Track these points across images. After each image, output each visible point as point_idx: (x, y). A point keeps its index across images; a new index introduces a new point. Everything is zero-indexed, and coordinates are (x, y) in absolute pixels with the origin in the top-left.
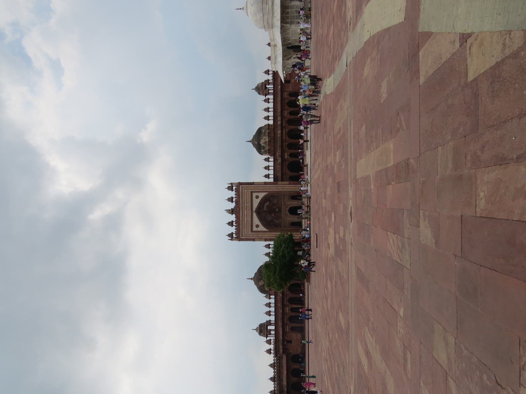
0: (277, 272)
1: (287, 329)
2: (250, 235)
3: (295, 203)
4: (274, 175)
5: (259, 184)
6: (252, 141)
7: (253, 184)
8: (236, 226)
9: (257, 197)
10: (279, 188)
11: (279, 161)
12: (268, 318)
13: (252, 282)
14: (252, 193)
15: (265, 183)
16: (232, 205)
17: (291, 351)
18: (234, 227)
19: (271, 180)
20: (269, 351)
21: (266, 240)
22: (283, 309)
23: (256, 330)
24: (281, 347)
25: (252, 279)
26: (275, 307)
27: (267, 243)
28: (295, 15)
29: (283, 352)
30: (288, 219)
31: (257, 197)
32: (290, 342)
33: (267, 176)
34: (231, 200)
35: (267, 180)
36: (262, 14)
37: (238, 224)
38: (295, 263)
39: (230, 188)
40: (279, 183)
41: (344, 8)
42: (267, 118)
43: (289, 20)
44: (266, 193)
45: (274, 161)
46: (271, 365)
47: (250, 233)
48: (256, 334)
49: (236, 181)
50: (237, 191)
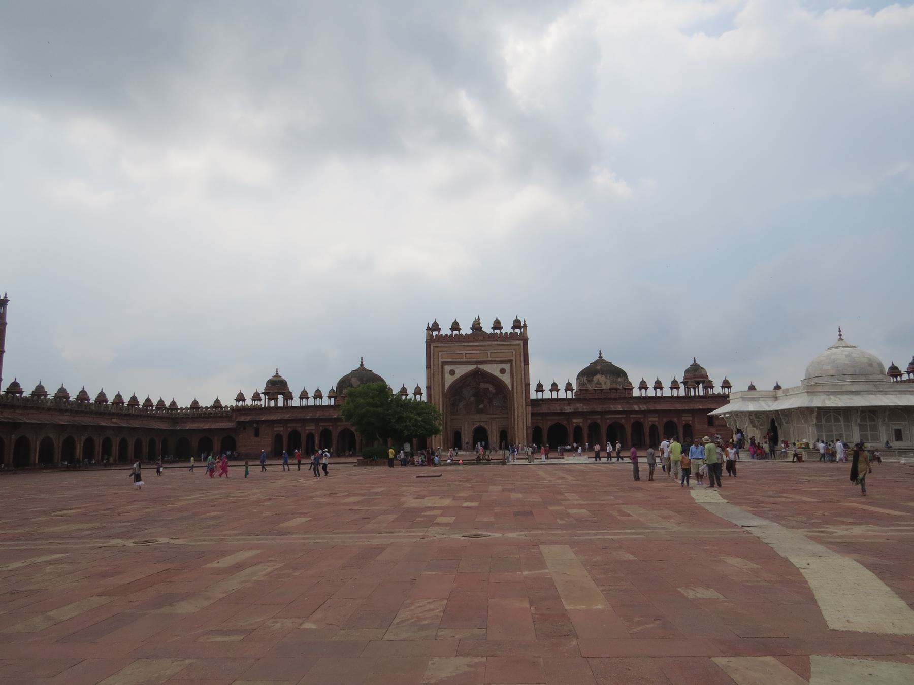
1: (279, 429)
3: (494, 437)
4: (543, 400)
6: (601, 360)
8: (451, 335)
9: (503, 371)
11: (568, 409)
12: (296, 394)
13: (356, 366)
14: (510, 361)
15: (527, 385)
16: (487, 328)
19: (533, 395)
20: (240, 398)
21: (429, 388)
22: (313, 420)
23: (277, 375)
24: (248, 418)
25: (362, 365)
26: (315, 407)
27: (424, 391)
28: (835, 433)
29: (239, 423)
31: (503, 371)
32: (257, 434)
33: (540, 388)
34: (497, 325)
35: (533, 387)
36: (832, 373)
37: (456, 339)
38: (389, 440)
39: (517, 324)
40: (529, 409)
41: (849, 520)
42: (643, 386)
43: (823, 422)
44: (510, 386)
45: (566, 400)
46: (217, 402)
47: (441, 360)
48: (270, 376)
49: (529, 335)
50: (513, 336)
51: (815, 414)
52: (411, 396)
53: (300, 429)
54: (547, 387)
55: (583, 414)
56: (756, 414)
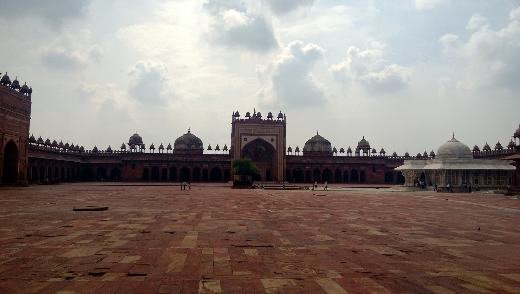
6: (318, 136)
7: (285, 137)
9: (272, 140)
14: (277, 135)
15: (285, 148)
31: (272, 140)
34: (270, 115)
39: (280, 115)
44: (276, 148)
47: (240, 133)
49: (287, 121)
55: (311, 164)
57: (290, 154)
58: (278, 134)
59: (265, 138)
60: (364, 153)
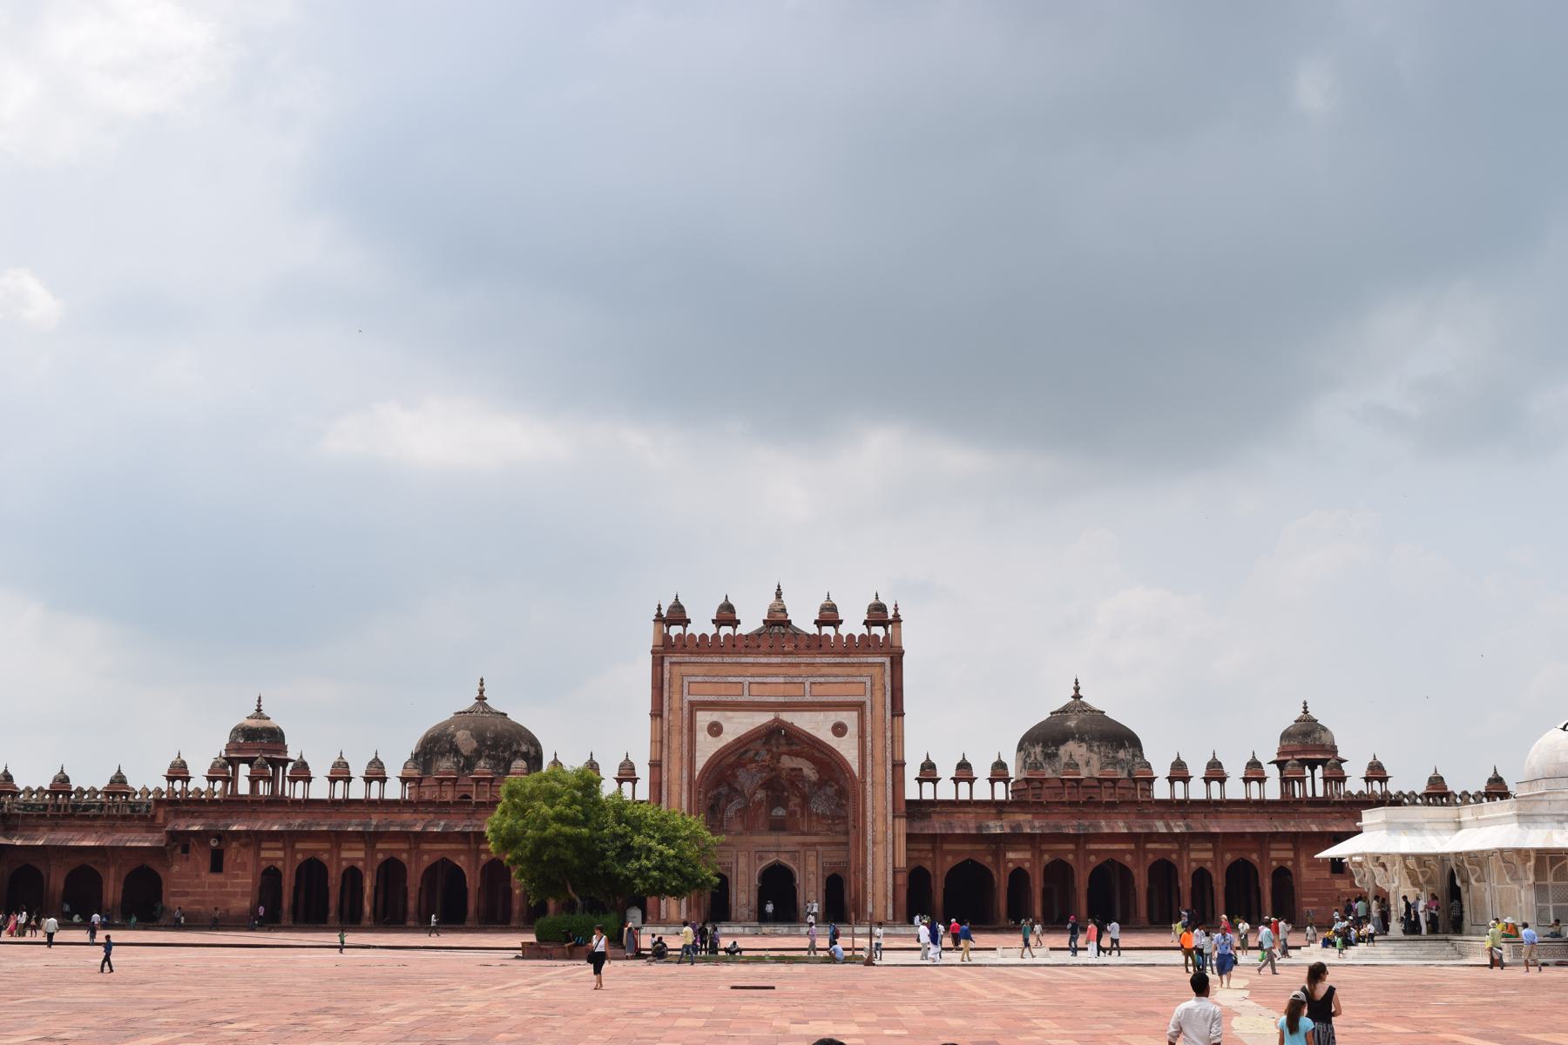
0: (567, 830)
1: (273, 854)
2: (676, 697)
4: (934, 803)
5: (897, 740)
7: (897, 711)
8: (716, 636)
9: (839, 729)
10: (880, 827)
11: (995, 827)
12: (320, 770)
13: (468, 702)
14: (859, 706)
15: (898, 766)
16: (804, 620)
17: (176, 868)
18: (711, 630)
19: (912, 792)
20: (179, 772)
21: (655, 765)
25: (481, 698)
27: (643, 772)
29: (174, 835)
30: (742, 861)
31: (839, 729)
32: (217, 866)
33: (928, 772)
34: (829, 616)
35: (912, 771)
37: (729, 646)
39: (877, 615)
40: (902, 825)
43: (1550, 880)
44: (855, 767)
46: (119, 779)
47: (687, 698)
50: (867, 644)
51: (1532, 863)
52: (608, 788)
53: (325, 857)
54: (946, 771)
55: (1031, 840)
56: (1419, 858)
57: (928, 792)
58: (867, 699)
59: (807, 722)
60: (253, 781)
